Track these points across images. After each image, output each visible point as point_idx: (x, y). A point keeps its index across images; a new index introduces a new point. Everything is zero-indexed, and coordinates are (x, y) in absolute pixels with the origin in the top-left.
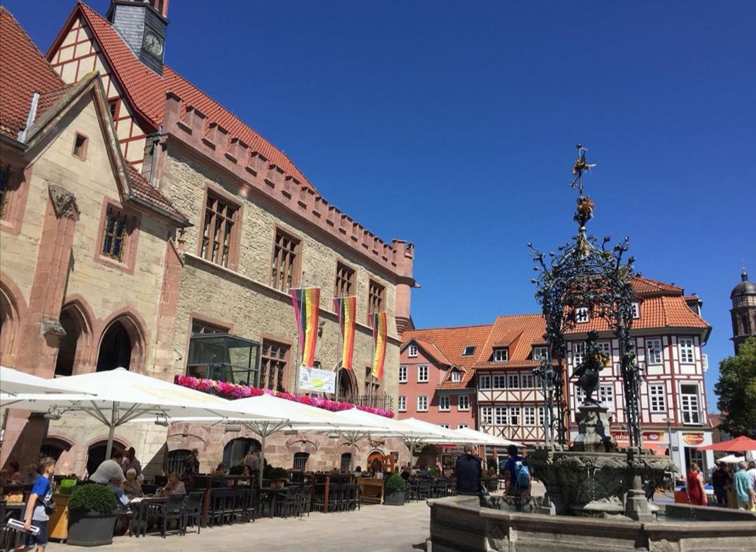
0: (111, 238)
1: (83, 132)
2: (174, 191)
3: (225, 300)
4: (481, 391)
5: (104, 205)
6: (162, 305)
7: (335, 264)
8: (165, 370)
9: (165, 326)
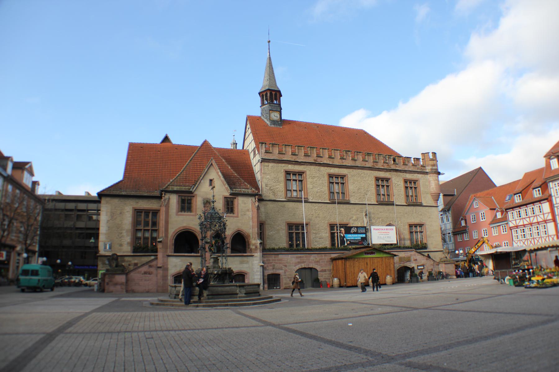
0: (229, 207)
1: (211, 178)
2: (268, 178)
4: (511, 221)
5: (223, 198)
6: (253, 225)
7: (374, 179)
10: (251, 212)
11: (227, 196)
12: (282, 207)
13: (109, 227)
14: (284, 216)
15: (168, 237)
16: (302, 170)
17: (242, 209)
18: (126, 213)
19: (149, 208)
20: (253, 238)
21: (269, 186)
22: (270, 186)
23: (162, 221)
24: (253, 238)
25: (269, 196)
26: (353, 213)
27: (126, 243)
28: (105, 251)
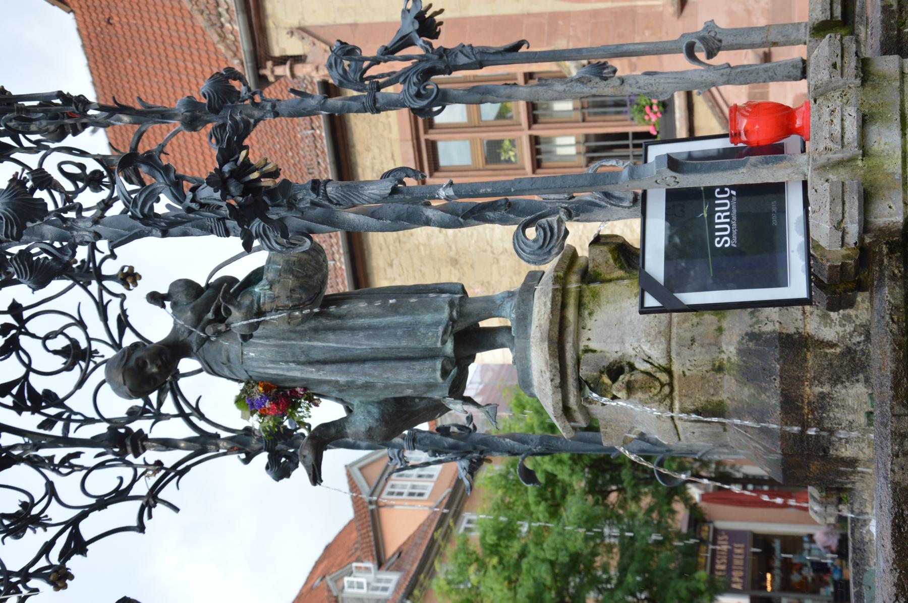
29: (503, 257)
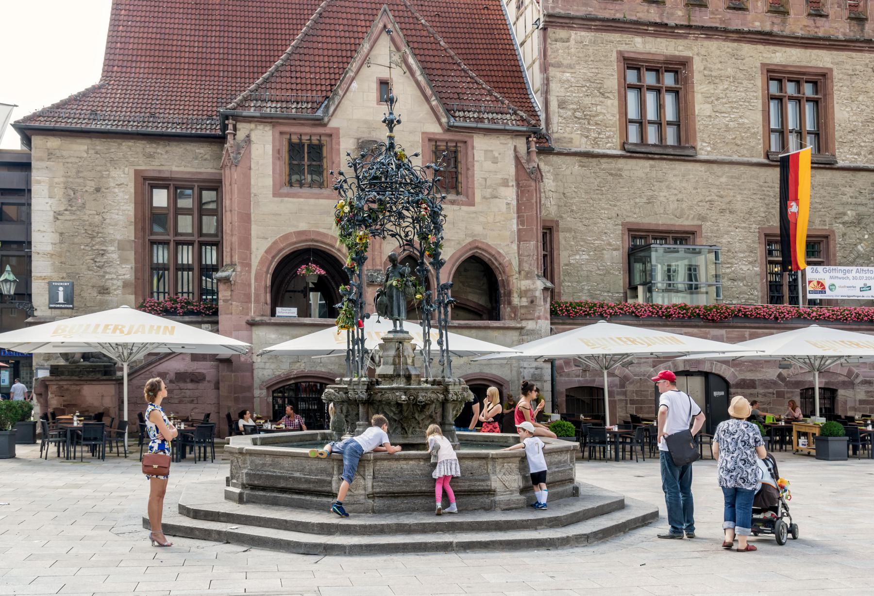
2: (568, 81)
3: (680, 196)
6: (519, 230)
8: (532, 302)
9: (526, 254)
10: (514, 190)
11: (433, 133)
12: (611, 174)
13: (61, 234)
14: (618, 204)
15: (249, 265)
16: (677, 53)
17: (486, 179)
18: (116, 190)
19: (189, 173)
20: (520, 272)
21: (571, 106)
22: (575, 107)
23: (228, 214)
24: (520, 272)
25: (572, 139)
26: (845, 199)
27: (120, 283)
28: (51, 308)
29: (100, 218)
